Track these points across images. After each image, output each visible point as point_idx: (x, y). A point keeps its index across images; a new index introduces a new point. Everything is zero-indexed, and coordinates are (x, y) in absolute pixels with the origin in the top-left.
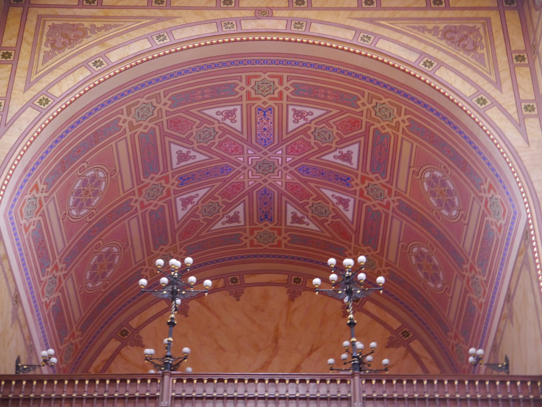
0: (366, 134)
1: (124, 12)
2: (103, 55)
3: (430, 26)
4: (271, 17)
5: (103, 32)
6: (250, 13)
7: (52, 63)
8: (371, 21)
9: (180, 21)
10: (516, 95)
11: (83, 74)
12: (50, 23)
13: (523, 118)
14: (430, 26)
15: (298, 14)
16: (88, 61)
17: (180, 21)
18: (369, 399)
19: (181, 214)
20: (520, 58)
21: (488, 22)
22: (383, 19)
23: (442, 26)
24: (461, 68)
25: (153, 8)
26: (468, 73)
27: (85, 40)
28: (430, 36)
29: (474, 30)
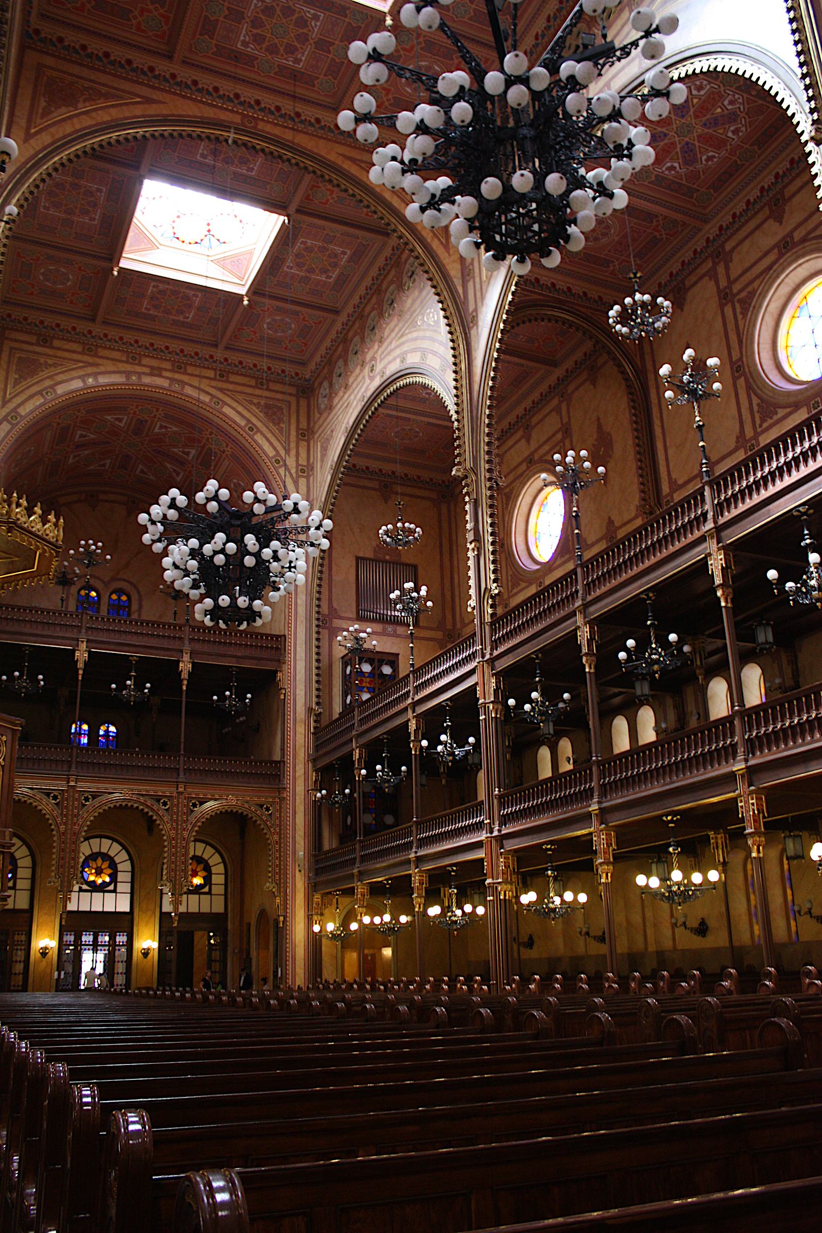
0: (203, 447)
1: (66, 355)
2: (52, 387)
3: (256, 401)
4: (160, 376)
5: (52, 369)
6: (147, 370)
7: (19, 388)
8: (221, 390)
9: (102, 369)
10: (297, 460)
11: (39, 401)
12: (18, 355)
13: (298, 476)
14: (256, 401)
15: (177, 376)
16: (42, 390)
17: (102, 369)
18: (193, 639)
19: (71, 461)
20: (303, 435)
21: (289, 402)
22: (228, 390)
23: (263, 402)
24: (269, 435)
25: (85, 354)
26: (273, 440)
27: (41, 373)
28: (254, 408)
29: (281, 409)
